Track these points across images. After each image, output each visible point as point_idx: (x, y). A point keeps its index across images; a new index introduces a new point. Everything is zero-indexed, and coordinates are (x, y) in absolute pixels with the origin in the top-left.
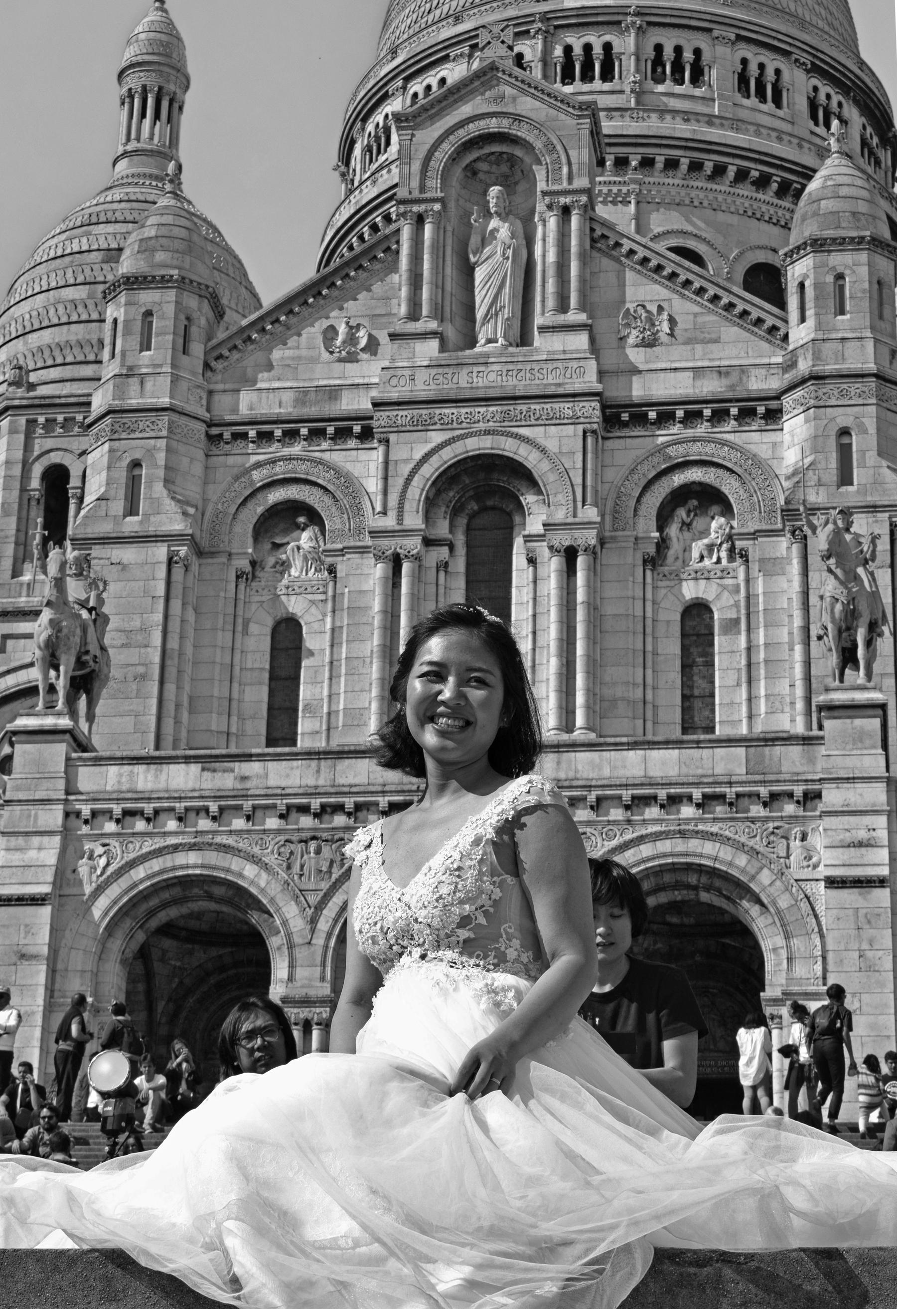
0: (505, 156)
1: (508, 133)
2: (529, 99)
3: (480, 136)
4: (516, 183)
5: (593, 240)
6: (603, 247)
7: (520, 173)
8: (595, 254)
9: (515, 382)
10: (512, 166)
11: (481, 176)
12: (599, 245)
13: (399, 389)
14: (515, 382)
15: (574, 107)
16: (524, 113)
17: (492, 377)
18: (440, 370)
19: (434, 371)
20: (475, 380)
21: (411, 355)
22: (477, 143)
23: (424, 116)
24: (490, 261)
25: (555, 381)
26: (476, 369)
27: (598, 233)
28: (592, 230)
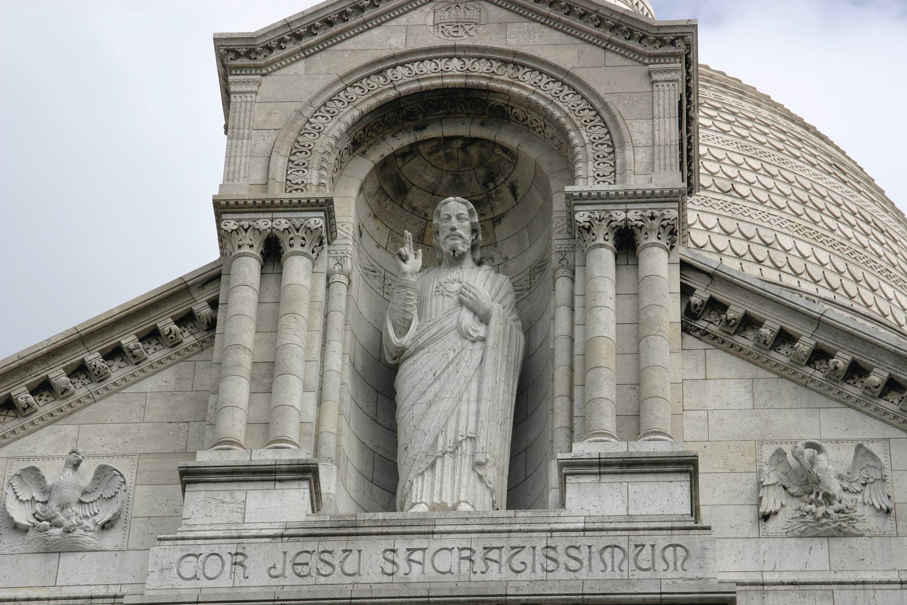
0: (474, 151)
1: (488, 91)
2: (536, 26)
3: (421, 96)
4: (497, 220)
5: (690, 314)
6: (714, 329)
7: (507, 194)
8: (690, 340)
9: (507, 574)
10: (491, 177)
11: (416, 198)
12: (702, 324)
13: (204, 583)
14: (507, 574)
15: (640, 40)
16: (525, 50)
17: (445, 561)
18: (311, 545)
19: (293, 547)
20: (403, 567)
21: (236, 517)
22: (410, 116)
23: (291, 48)
24: (439, 345)
25: (609, 574)
26: (401, 545)
27: (700, 296)
28: (686, 291)
